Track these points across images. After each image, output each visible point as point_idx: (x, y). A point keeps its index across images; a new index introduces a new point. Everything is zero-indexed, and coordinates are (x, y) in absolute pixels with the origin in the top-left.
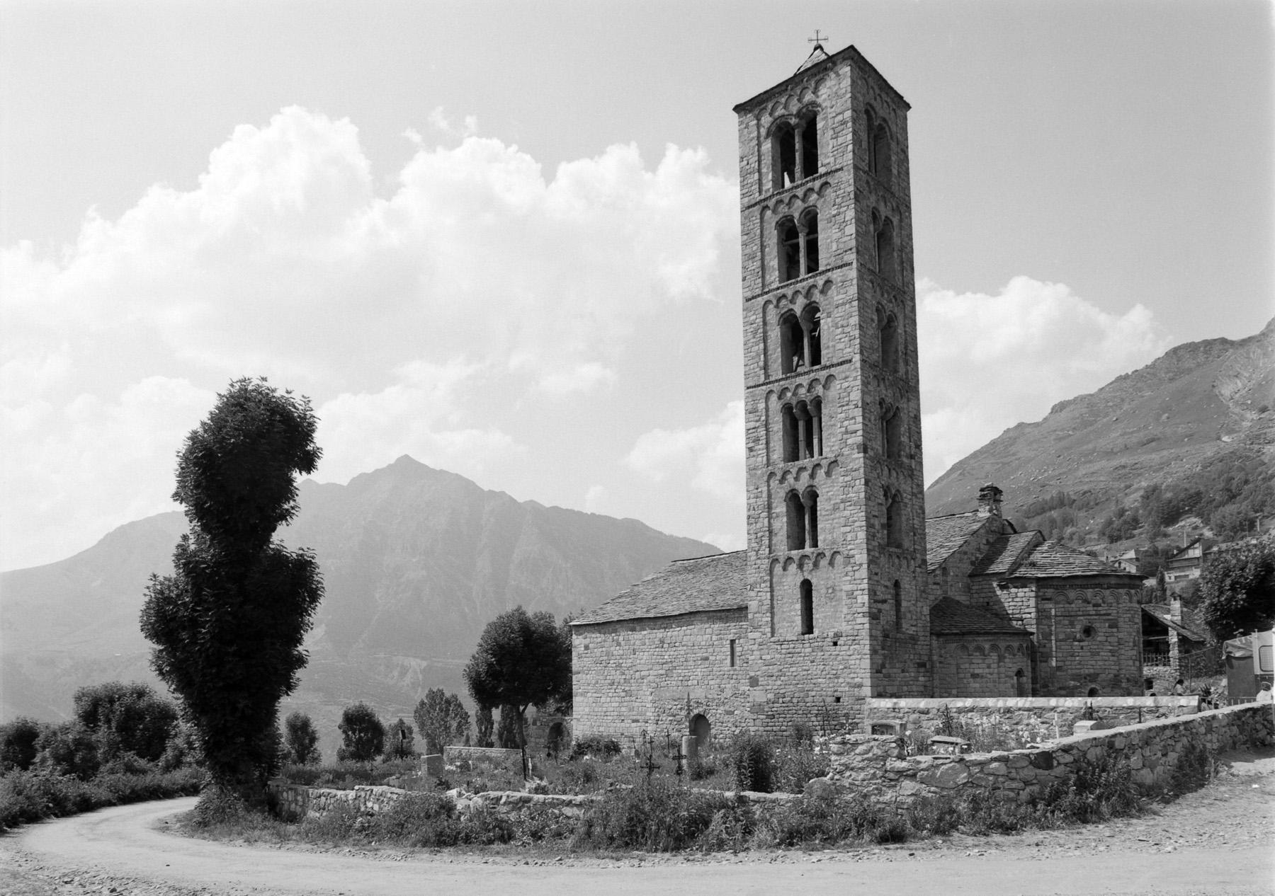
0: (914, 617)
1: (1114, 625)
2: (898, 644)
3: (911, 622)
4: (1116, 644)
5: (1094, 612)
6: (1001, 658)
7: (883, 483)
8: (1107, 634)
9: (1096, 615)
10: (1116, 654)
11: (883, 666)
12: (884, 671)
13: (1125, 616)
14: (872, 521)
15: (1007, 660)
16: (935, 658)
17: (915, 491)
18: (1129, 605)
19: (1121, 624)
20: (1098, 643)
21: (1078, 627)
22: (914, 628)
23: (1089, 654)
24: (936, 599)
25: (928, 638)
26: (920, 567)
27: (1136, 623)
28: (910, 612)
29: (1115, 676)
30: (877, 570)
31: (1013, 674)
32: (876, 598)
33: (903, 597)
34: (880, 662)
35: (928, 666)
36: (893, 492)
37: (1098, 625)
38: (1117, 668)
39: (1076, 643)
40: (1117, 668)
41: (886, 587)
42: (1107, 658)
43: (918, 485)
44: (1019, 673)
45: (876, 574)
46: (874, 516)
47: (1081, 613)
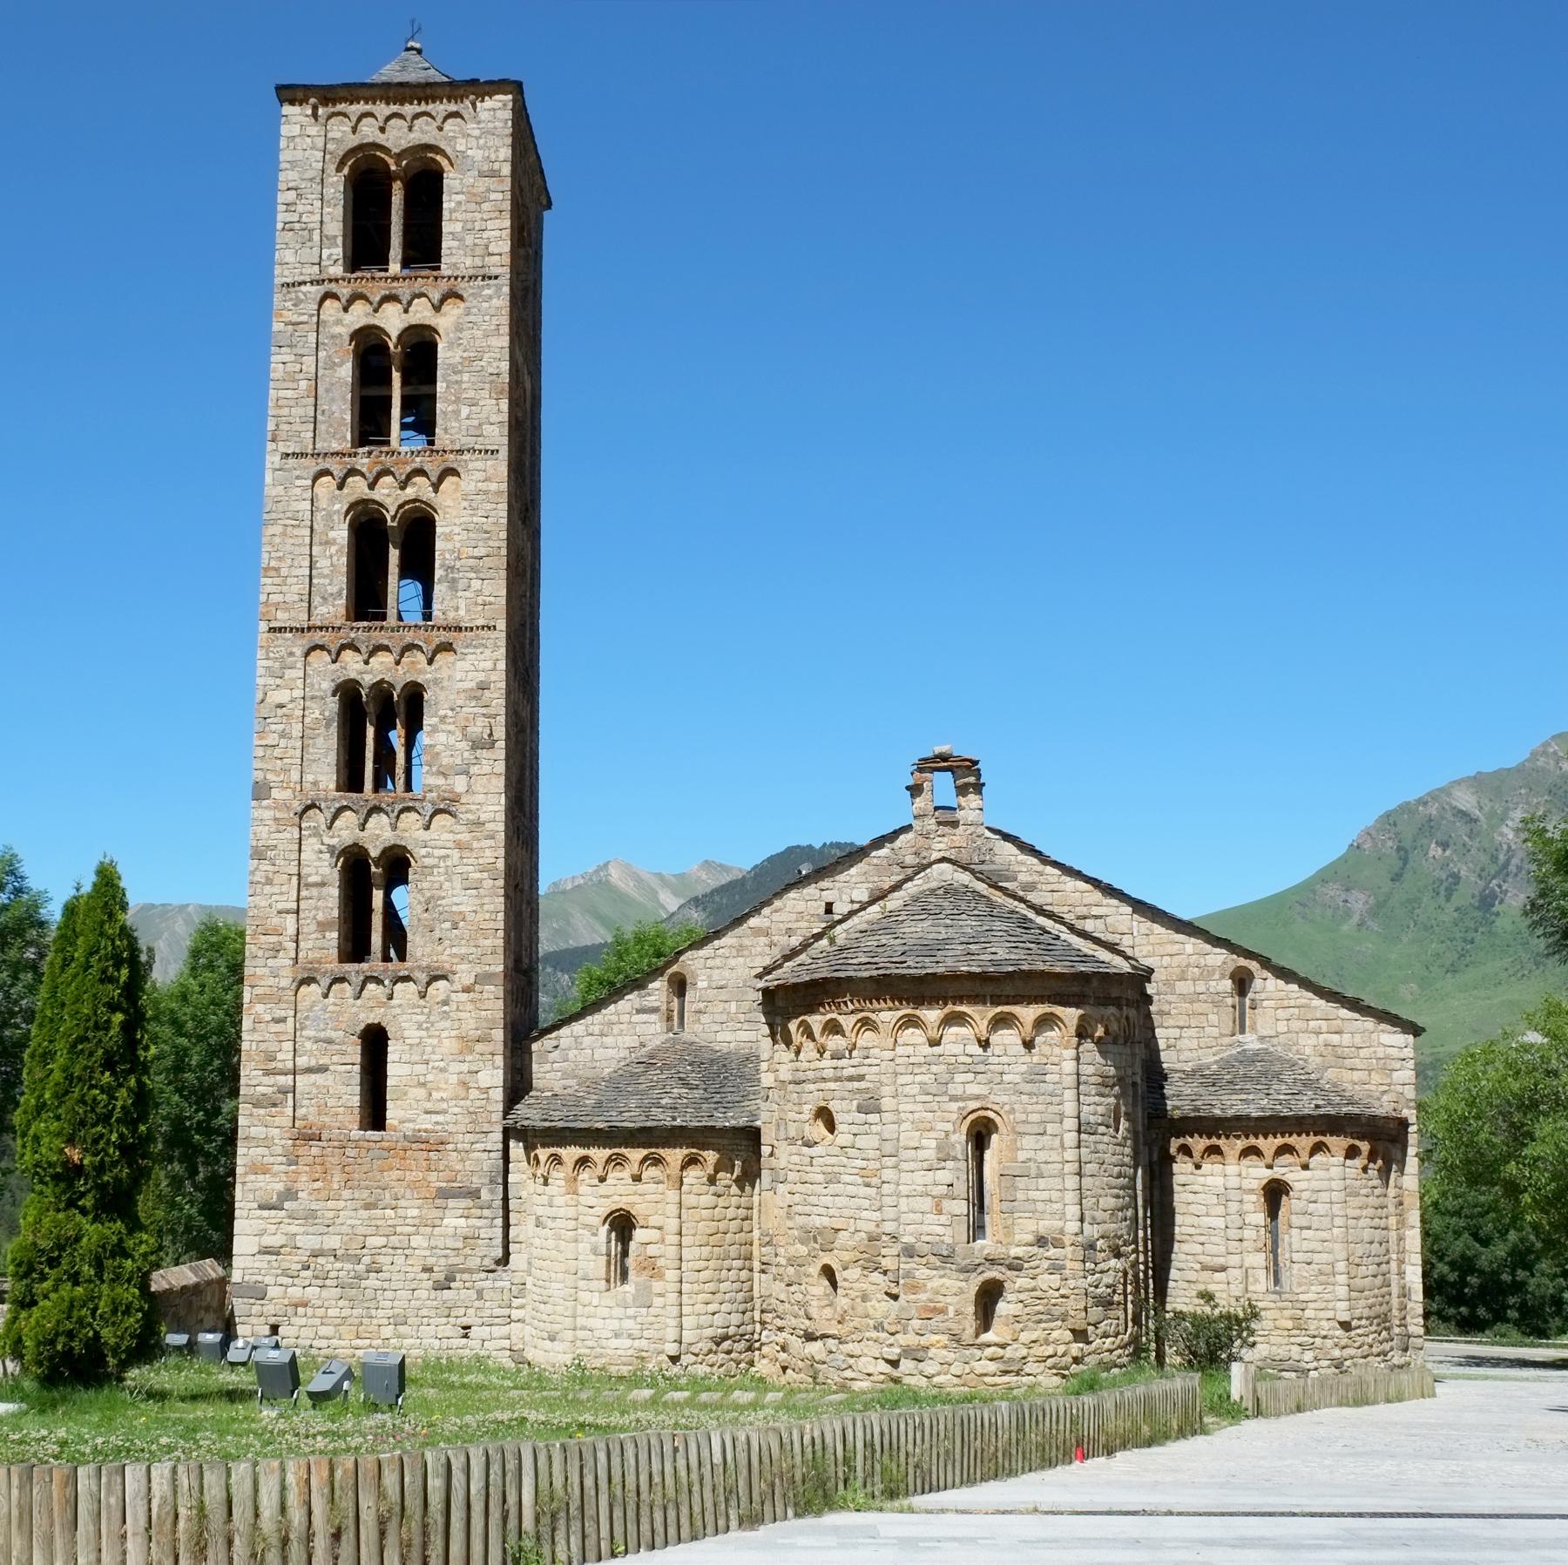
0: (436, 1095)
1: (870, 1106)
2: (350, 1152)
3: (429, 1106)
4: (872, 1154)
5: (829, 1073)
6: (572, 1183)
7: (334, 841)
8: (855, 1129)
9: (838, 1079)
10: (875, 1181)
11: (290, 1194)
12: (287, 1205)
13: (902, 1080)
14: (276, 921)
15: (583, 1189)
16: (511, 1178)
17: (465, 837)
18: (927, 1050)
19: (887, 1103)
20: (836, 1150)
21: (807, 1107)
22: (440, 1118)
23: (821, 1178)
24: (643, 1045)
25: (499, 1136)
26: (467, 990)
27: (954, 1099)
28: (424, 1085)
29: (872, 1238)
30: (283, 1014)
31: (597, 1221)
32: (280, 1065)
33: (390, 1058)
34: (280, 1187)
35: (485, 1194)
36: (374, 853)
37: (834, 1106)
38: (877, 1216)
39: (805, 1149)
40: (877, 1216)
41: (330, 1041)
42: (851, 1190)
43: (479, 824)
44: (622, 1225)
45: (283, 1020)
46: (279, 912)
47: (810, 1074)
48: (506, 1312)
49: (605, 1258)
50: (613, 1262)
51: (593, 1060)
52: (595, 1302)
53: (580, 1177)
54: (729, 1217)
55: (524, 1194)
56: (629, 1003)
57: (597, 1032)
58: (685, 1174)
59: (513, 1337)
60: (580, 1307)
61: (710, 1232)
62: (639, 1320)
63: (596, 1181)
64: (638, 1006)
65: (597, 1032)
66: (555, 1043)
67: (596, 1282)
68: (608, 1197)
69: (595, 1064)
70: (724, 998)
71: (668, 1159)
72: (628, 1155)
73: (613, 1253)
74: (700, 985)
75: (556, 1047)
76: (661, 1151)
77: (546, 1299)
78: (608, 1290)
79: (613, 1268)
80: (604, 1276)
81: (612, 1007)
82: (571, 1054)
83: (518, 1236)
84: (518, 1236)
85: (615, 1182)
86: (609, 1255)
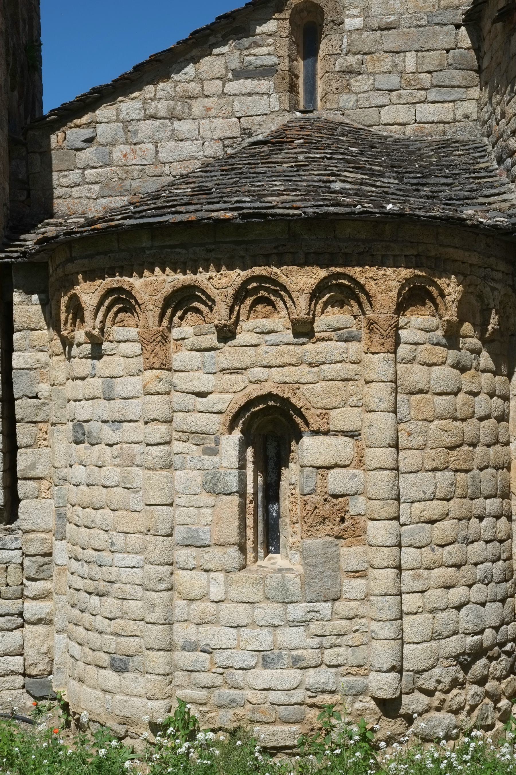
24: (246, 132)
48: (14, 606)
49: (236, 500)
50: (250, 507)
51: (157, 162)
52: (216, 592)
53: (175, 333)
54: (480, 412)
55: (44, 389)
56: (221, 61)
57: (163, 111)
58: (402, 321)
59: (29, 652)
60: (180, 603)
61: (449, 441)
62: (315, 627)
63: (212, 340)
64: (235, 64)
65: (163, 111)
66: (87, 133)
67: (217, 551)
68: (238, 371)
69: (160, 169)
70: (393, 46)
71: (371, 287)
72: (283, 279)
73: (250, 489)
74: (349, 23)
75: (90, 140)
76: (356, 272)
77: (102, 586)
78: (243, 567)
79: (250, 521)
80: (234, 537)
81: (190, 69)
82: (117, 153)
83: (33, 466)
84: (33, 466)
85: (254, 339)
86: (242, 493)
